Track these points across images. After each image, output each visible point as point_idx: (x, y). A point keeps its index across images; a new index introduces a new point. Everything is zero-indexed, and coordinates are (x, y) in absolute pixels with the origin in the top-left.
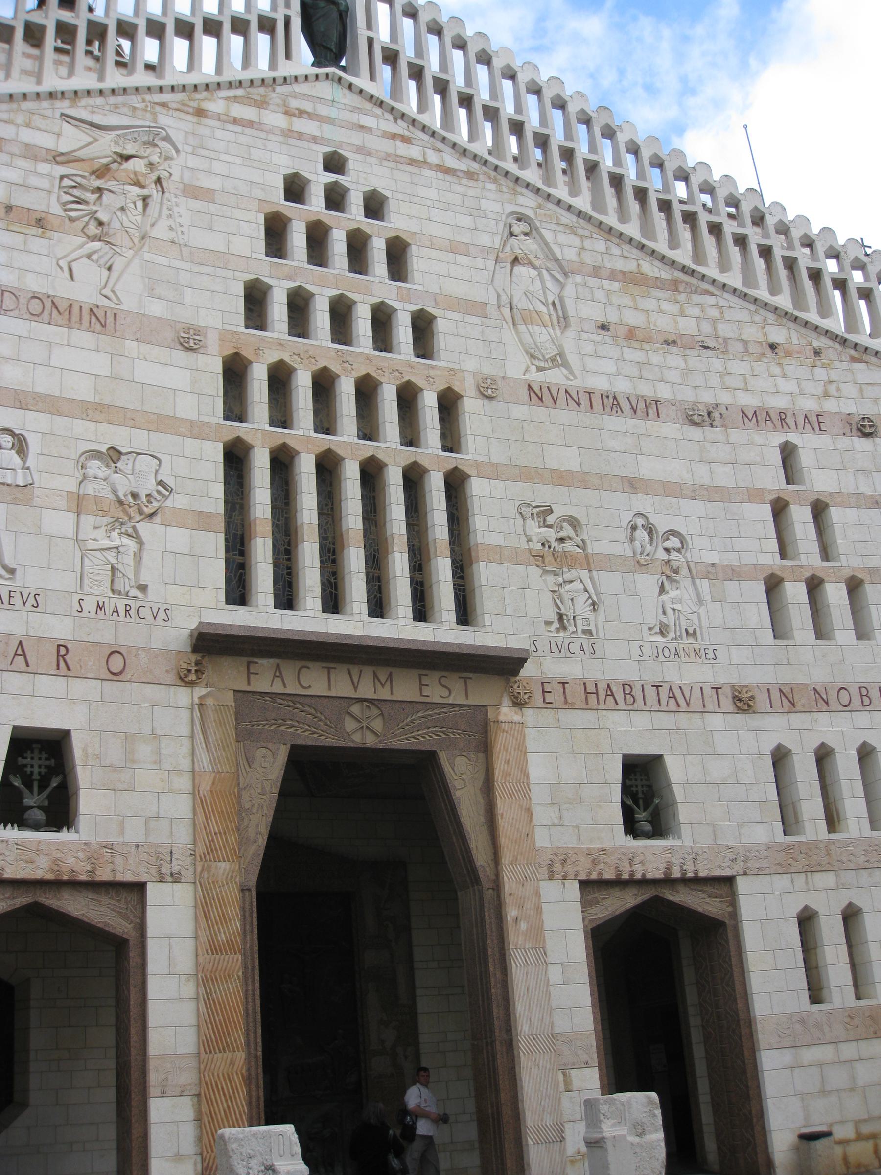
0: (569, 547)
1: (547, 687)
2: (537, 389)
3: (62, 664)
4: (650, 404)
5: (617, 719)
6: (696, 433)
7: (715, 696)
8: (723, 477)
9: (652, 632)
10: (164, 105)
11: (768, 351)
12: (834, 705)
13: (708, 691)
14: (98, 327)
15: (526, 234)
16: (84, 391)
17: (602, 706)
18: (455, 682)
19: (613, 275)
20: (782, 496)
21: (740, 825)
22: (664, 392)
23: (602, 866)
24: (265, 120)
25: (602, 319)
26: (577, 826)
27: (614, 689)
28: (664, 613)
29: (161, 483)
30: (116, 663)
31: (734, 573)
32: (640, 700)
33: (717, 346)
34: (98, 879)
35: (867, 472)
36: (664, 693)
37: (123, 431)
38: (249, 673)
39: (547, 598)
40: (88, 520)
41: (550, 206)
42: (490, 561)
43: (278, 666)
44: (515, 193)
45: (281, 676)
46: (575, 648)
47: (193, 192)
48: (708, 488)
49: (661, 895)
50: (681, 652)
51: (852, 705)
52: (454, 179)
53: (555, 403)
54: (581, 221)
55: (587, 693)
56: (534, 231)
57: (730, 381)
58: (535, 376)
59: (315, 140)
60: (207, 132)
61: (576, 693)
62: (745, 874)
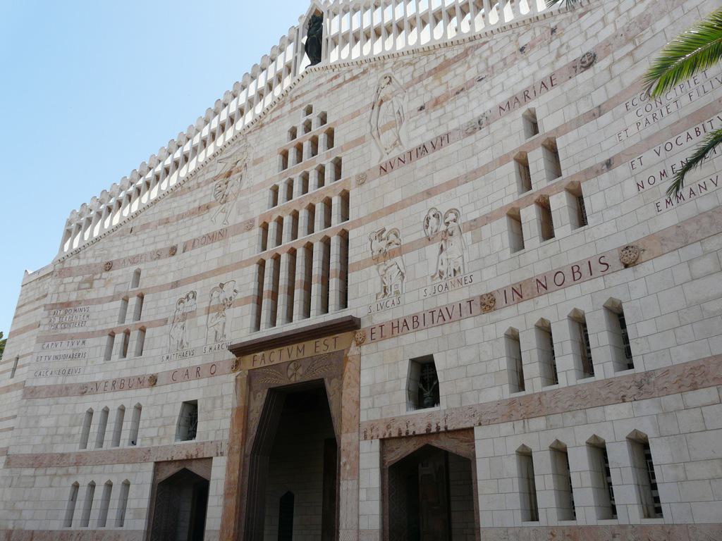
0: (393, 246)
6: (471, 139)
8: (485, 158)
10: (250, 132)
11: (519, 55)
12: (551, 286)
13: (465, 305)
14: (220, 238)
16: (214, 266)
18: (330, 340)
19: (430, 74)
20: (521, 150)
21: (479, 391)
22: (453, 125)
25: (422, 104)
26: (381, 408)
28: (442, 264)
29: (235, 291)
31: (488, 219)
36: (436, 315)
37: (223, 276)
39: (378, 281)
46: (389, 304)
47: (255, 162)
49: (430, 443)
50: (449, 285)
58: (386, 159)
59: (301, 106)
60: (263, 132)
62: (480, 424)
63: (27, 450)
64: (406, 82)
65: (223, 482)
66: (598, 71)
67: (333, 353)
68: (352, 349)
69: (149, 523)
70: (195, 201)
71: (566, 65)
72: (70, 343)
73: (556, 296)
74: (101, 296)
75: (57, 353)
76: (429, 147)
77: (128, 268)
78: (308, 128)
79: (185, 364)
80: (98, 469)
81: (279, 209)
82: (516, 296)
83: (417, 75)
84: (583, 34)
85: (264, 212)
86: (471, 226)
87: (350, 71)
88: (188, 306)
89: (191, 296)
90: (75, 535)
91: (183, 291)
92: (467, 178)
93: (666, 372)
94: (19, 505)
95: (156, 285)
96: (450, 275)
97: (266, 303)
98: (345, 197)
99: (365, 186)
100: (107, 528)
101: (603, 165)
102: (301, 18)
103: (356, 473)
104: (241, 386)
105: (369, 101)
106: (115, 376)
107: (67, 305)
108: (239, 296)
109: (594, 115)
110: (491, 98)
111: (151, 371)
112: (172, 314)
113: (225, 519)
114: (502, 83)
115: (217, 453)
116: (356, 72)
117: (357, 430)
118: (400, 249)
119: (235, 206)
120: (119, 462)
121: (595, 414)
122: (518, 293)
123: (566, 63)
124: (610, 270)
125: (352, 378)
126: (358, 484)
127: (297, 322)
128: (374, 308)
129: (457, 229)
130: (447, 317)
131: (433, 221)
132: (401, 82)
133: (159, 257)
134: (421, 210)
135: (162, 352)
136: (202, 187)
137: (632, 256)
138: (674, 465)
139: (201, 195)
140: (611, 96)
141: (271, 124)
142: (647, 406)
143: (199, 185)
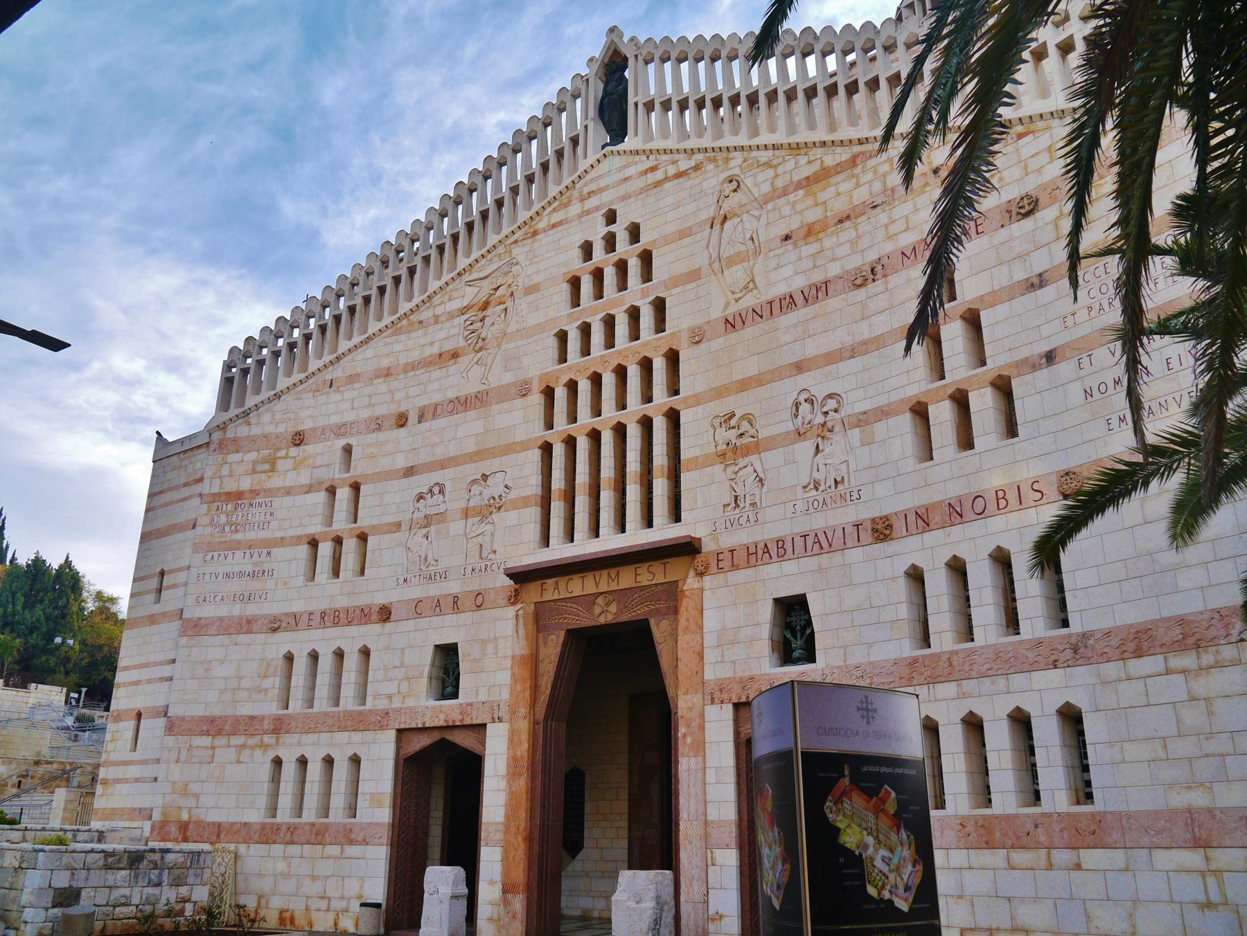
1: (721, 557)
2: (731, 319)
3: (455, 607)
4: (820, 287)
5: (771, 570)
6: (861, 294)
7: (856, 532)
9: (807, 490)
10: (516, 242)
12: (968, 515)
13: (849, 529)
15: (735, 191)
16: (470, 446)
17: (760, 562)
18: (657, 567)
19: (799, 186)
21: (870, 645)
22: (834, 270)
23: (749, 691)
24: (569, 215)
26: (734, 662)
27: (769, 546)
28: (818, 470)
29: (506, 487)
30: (479, 602)
31: (884, 413)
32: (789, 551)
33: (884, 200)
34: (465, 723)
35: (1022, 257)
36: (810, 540)
38: (542, 590)
39: (727, 484)
40: (470, 521)
41: (755, 153)
42: (688, 470)
43: (557, 582)
44: (727, 160)
45: (558, 589)
47: (529, 291)
48: (864, 343)
50: (828, 501)
51: (986, 511)
52: (685, 178)
53: (744, 323)
54: (776, 152)
55: (749, 554)
56: (741, 184)
57: (893, 229)
58: (734, 308)
59: (597, 209)
60: (537, 244)
61: (741, 556)
63: (197, 711)
64: (763, 192)
65: (505, 757)
66: (1040, 224)
67: (662, 584)
68: (689, 580)
69: (394, 814)
70: (432, 344)
71: (998, 206)
72: (248, 555)
73: (974, 528)
74: (289, 483)
75: (228, 569)
76: (799, 299)
77: (330, 443)
78: (610, 242)
79: (434, 590)
80: (312, 738)
81: (570, 368)
82: (920, 523)
83: (780, 183)
84: (1023, 164)
85: (546, 371)
86: (860, 420)
87: (675, 162)
88: (432, 505)
89: (436, 489)
90: (284, 827)
91: (422, 482)
92: (854, 351)
93: (1108, 634)
94: (194, 788)
95: (378, 470)
96: (830, 487)
97: (557, 508)
98: (673, 358)
99: (703, 346)
100: (331, 819)
101: (1041, 357)
102: (591, 60)
103: (700, 747)
104: (525, 625)
105: (706, 215)
106: (324, 605)
107: (239, 495)
108: (513, 494)
109: (1032, 285)
110: (890, 237)
111: (380, 599)
112: (408, 516)
113: (511, 808)
114: (907, 217)
115: (493, 718)
116: (684, 165)
117: (701, 691)
118: (757, 443)
119: (498, 357)
120: (341, 729)
121: (1018, 680)
122: (923, 519)
123: (997, 203)
124: (1044, 501)
125: (690, 620)
126: (704, 761)
127: (606, 537)
128: (721, 525)
129: (839, 422)
130: (825, 544)
131: (804, 408)
132: (756, 192)
133: (379, 428)
134: (789, 389)
135: (396, 571)
136: (442, 322)
137: (1074, 485)
138: (1110, 744)
139: (442, 335)
140: (1056, 263)
141: (550, 232)
142: (1083, 674)
143: (436, 320)
